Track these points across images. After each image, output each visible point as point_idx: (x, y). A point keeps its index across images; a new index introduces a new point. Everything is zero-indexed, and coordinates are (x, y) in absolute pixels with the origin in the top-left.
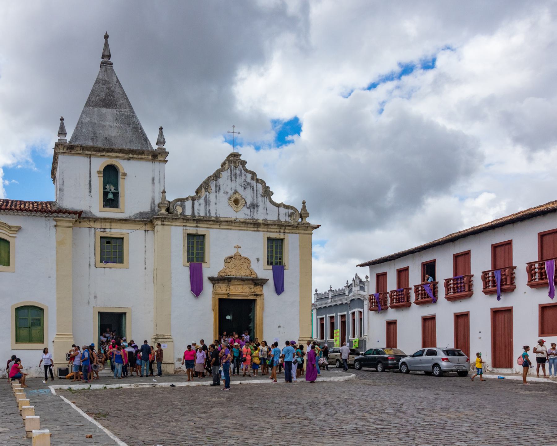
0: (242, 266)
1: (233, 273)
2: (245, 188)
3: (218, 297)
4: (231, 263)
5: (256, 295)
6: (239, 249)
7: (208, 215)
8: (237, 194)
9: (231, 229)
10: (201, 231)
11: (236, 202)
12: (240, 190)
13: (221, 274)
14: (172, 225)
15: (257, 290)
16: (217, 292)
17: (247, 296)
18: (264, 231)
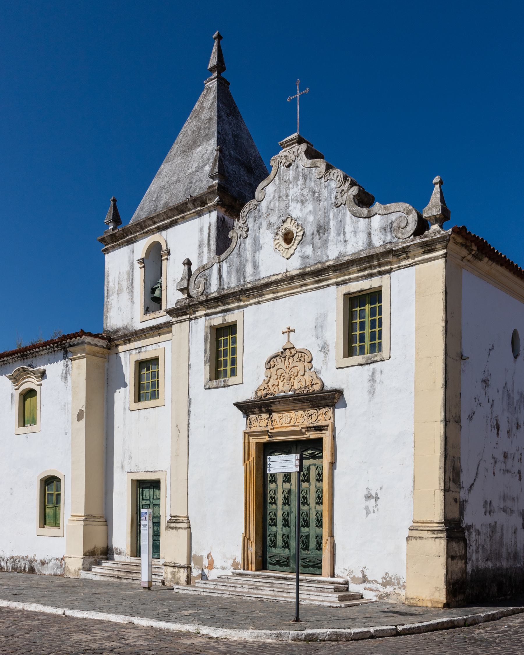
0: (295, 370)
1: (282, 388)
2: (303, 203)
3: (254, 441)
4: (276, 367)
5: (319, 428)
6: (291, 334)
7: (242, 282)
8: (289, 220)
9: (276, 298)
10: (230, 318)
11: (288, 238)
12: (296, 211)
13: (259, 394)
14: (190, 319)
15: (320, 416)
16: (253, 429)
17: (300, 432)
18: (338, 284)
